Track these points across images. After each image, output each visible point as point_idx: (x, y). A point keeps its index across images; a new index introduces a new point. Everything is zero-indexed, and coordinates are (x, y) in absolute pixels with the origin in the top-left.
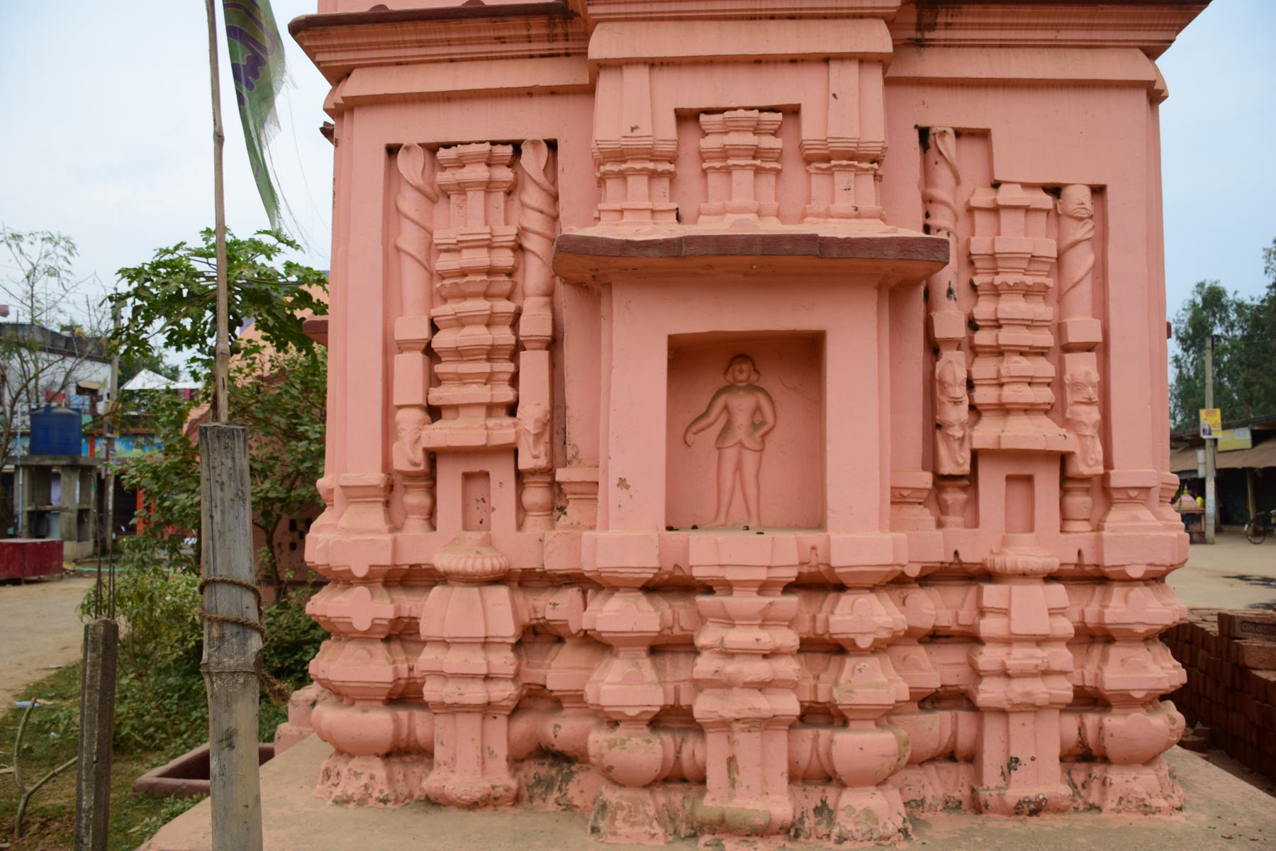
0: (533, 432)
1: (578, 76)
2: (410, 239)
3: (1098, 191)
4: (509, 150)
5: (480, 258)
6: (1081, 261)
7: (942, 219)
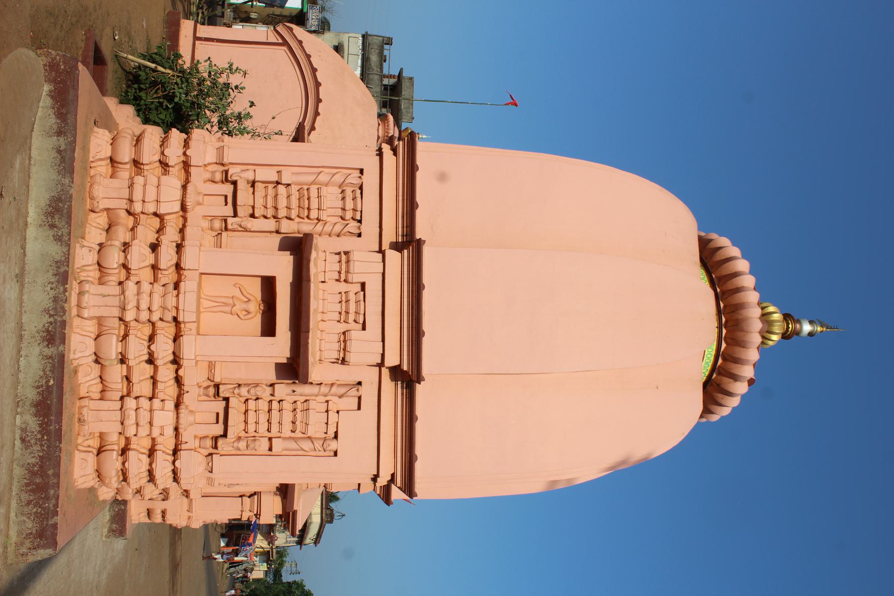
1: (385, 246)
2: (323, 178)
3: (336, 454)
4: (359, 218)
5: (314, 204)
6: (307, 445)
7: (324, 389)
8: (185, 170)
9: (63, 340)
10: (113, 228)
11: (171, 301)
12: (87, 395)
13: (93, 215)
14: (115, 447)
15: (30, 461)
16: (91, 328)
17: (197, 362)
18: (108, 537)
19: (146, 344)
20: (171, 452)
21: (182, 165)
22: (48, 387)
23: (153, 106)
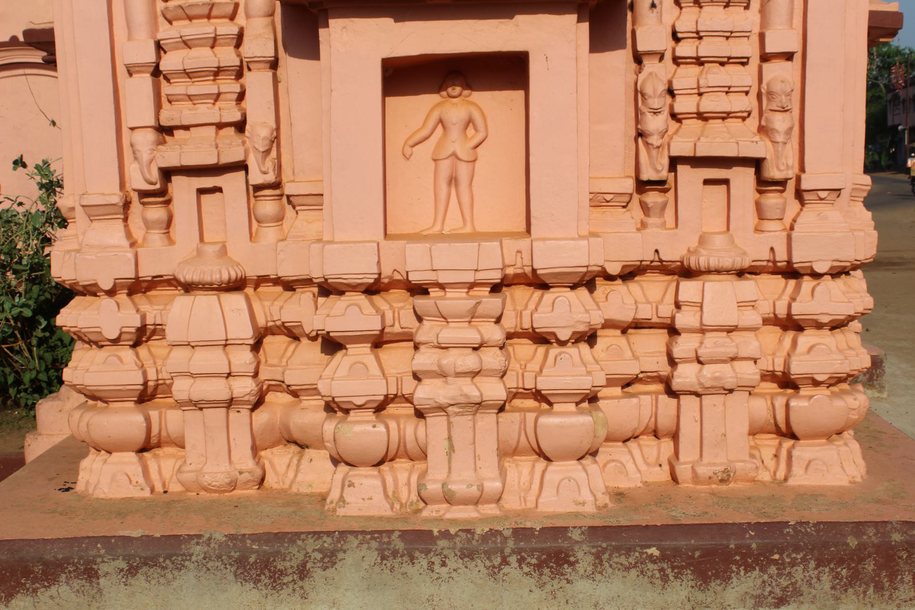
0: (262, 149)
8: (148, 289)
9: (559, 532)
10: (296, 435)
11: (456, 301)
12: (666, 467)
13: (270, 480)
14: (780, 402)
15: (827, 586)
16: (523, 470)
17: (593, 235)
18: (881, 388)
19: (555, 350)
20: (792, 283)
21: (138, 297)
22: (663, 558)
23: (48, 356)
